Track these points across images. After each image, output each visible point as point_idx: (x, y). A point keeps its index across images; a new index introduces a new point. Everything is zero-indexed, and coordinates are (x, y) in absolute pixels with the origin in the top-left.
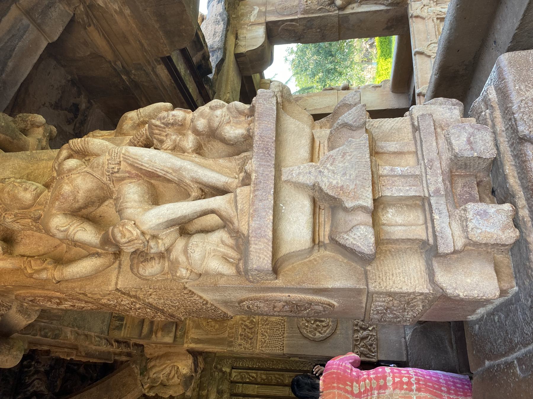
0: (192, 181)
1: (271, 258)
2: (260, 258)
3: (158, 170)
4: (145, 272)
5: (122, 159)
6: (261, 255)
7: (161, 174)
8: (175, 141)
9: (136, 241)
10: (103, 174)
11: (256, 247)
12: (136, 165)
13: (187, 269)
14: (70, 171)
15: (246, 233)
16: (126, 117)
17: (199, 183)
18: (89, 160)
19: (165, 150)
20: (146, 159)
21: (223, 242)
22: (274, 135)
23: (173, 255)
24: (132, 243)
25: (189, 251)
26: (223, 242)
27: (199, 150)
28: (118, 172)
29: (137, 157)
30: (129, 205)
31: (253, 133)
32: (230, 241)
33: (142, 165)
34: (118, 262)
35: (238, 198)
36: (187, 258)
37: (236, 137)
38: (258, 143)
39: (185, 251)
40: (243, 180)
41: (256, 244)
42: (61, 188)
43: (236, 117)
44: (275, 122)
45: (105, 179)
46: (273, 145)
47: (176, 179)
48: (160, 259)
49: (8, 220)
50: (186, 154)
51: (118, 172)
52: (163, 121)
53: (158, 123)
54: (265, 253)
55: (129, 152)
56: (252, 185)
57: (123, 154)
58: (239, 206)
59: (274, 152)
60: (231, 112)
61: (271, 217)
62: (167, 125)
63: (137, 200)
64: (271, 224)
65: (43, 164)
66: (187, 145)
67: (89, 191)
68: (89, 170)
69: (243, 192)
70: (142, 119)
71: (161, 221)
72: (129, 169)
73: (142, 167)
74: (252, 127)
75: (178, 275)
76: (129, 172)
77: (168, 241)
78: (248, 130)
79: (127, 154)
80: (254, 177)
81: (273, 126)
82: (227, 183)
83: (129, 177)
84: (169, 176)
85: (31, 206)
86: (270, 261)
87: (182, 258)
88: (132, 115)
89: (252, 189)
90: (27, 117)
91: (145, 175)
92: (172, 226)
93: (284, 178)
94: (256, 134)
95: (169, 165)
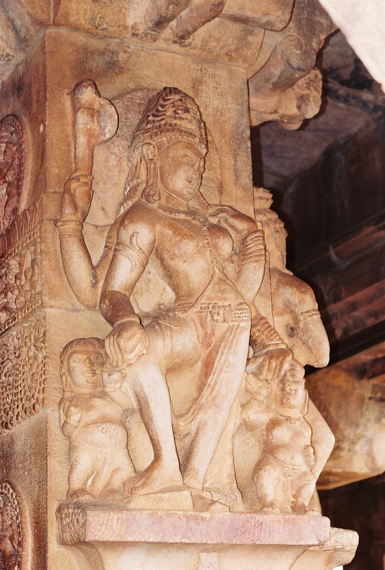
0: (200, 422)
1: (100, 540)
2: (101, 526)
3: (215, 376)
4: (74, 361)
5: (231, 324)
6: (104, 526)
7: (210, 379)
8: (259, 394)
9: (120, 357)
10: (209, 298)
11: (115, 521)
12: (223, 344)
13: (79, 422)
14: (216, 247)
15: (132, 505)
16: (305, 292)
17: (197, 433)
18: (233, 262)
19: (246, 378)
20: (231, 359)
21: (116, 470)
22: (263, 543)
23: (97, 402)
24: (118, 352)
25: (104, 425)
26: (116, 470)
27: (247, 426)
28: (213, 319)
29: (234, 346)
30: (168, 340)
31: (266, 513)
32: (117, 483)
33: (222, 354)
34: (82, 307)
35: (176, 494)
36: (95, 423)
37: (262, 486)
38: (253, 520)
39: (105, 420)
40: (202, 498)
41: (118, 520)
42: (191, 237)
43: (292, 486)
44: (282, 543)
45: (203, 301)
46: (249, 542)
47: (203, 401)
48: (93, 383)
49: (145, 148)
50: (240, 409)
51: (213, 319)
52: (288, 374)
53: (286, 366)
54: (106, 532)
55: (241, 333)
56: (193, 513)
57: (238, 325)
58: (166, 496)
59: (239, 542)
60: (299, 477)
61: (151, 540)
62: (283, 381)
63: (174, 350)
64: (143, 540)
65: (229, 161)
66: (252, 411)
67: (187, 277)
68: (216, 279)
69: (184, 500)
70: (301, 318)
71: (146, 390)
72: (218, 334)
73: (220, 353)
74: (274, 511)
75: (72, 409)
76: (213, 334)
77: (117, 395)
78: (272, 505)
79: (239, 330)
80: (205, 516)
81: (276, 540)
82: (197, 473)
83: (206, 333)
84: (206, 391)
85: (166, 187)
86: (97, 538)
87: (94, 415)
88: (308, 302)
89: (190, 513)
90: (316, 89)
91: (209, 355)
92: (139, 401)
93: (203, 555)
94: (265, 517)
95: (223, 391)
